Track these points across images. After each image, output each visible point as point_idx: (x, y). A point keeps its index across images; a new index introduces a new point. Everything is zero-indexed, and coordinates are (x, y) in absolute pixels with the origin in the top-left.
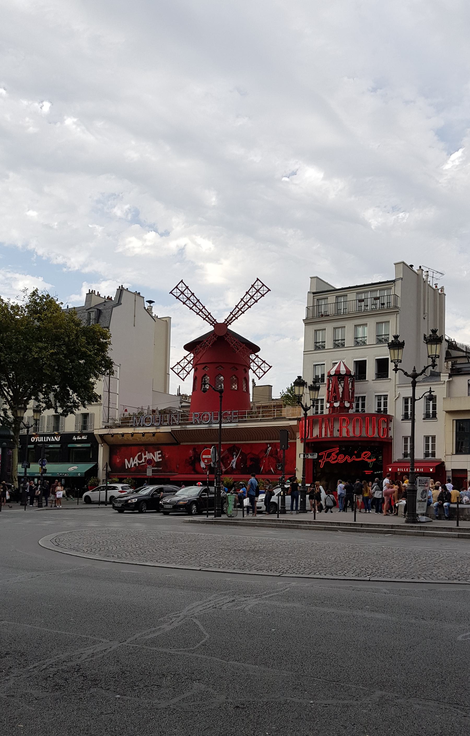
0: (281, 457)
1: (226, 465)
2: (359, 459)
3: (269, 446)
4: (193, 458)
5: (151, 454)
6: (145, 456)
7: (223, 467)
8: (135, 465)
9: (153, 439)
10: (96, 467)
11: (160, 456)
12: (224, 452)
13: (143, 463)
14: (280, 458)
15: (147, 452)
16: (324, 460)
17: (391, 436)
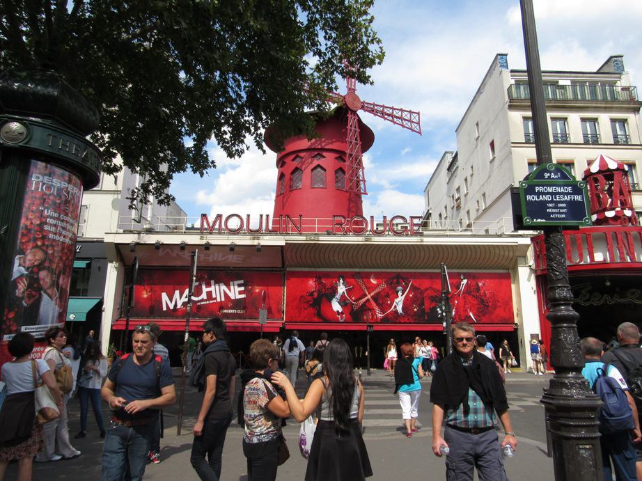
0: (485, 296)
3: (462, 277)
4: (316, 294)
5: (223, 287)
6: (209, 289)
9: (233, 260)
10: (101, 303)
12: (377, 286)
13: (202, 300)
15: (212, 282)
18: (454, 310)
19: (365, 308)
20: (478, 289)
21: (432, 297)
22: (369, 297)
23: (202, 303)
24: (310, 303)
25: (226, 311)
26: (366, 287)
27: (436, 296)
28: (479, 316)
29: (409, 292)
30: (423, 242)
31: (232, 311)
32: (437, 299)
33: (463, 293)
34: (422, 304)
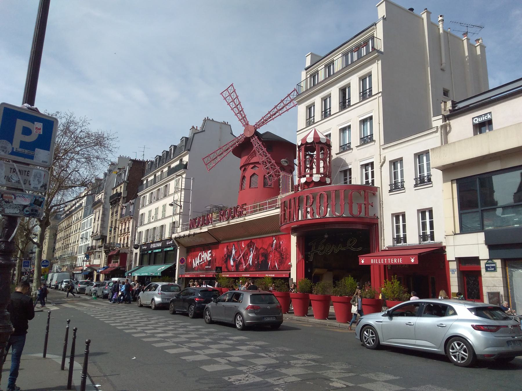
0: (283, 251)
1: (246, 261)
4: (226, 256)
8: (198, 263)
10: (175, 266)
11: (210, 255)
13: (202, 262)
16: (313, 252)
17: (375, 215)
20: (280, 247)
21: (262, 253)
22: (241, 255)
23: (201, 263)
28: (279, 266)
30: (245, 220)
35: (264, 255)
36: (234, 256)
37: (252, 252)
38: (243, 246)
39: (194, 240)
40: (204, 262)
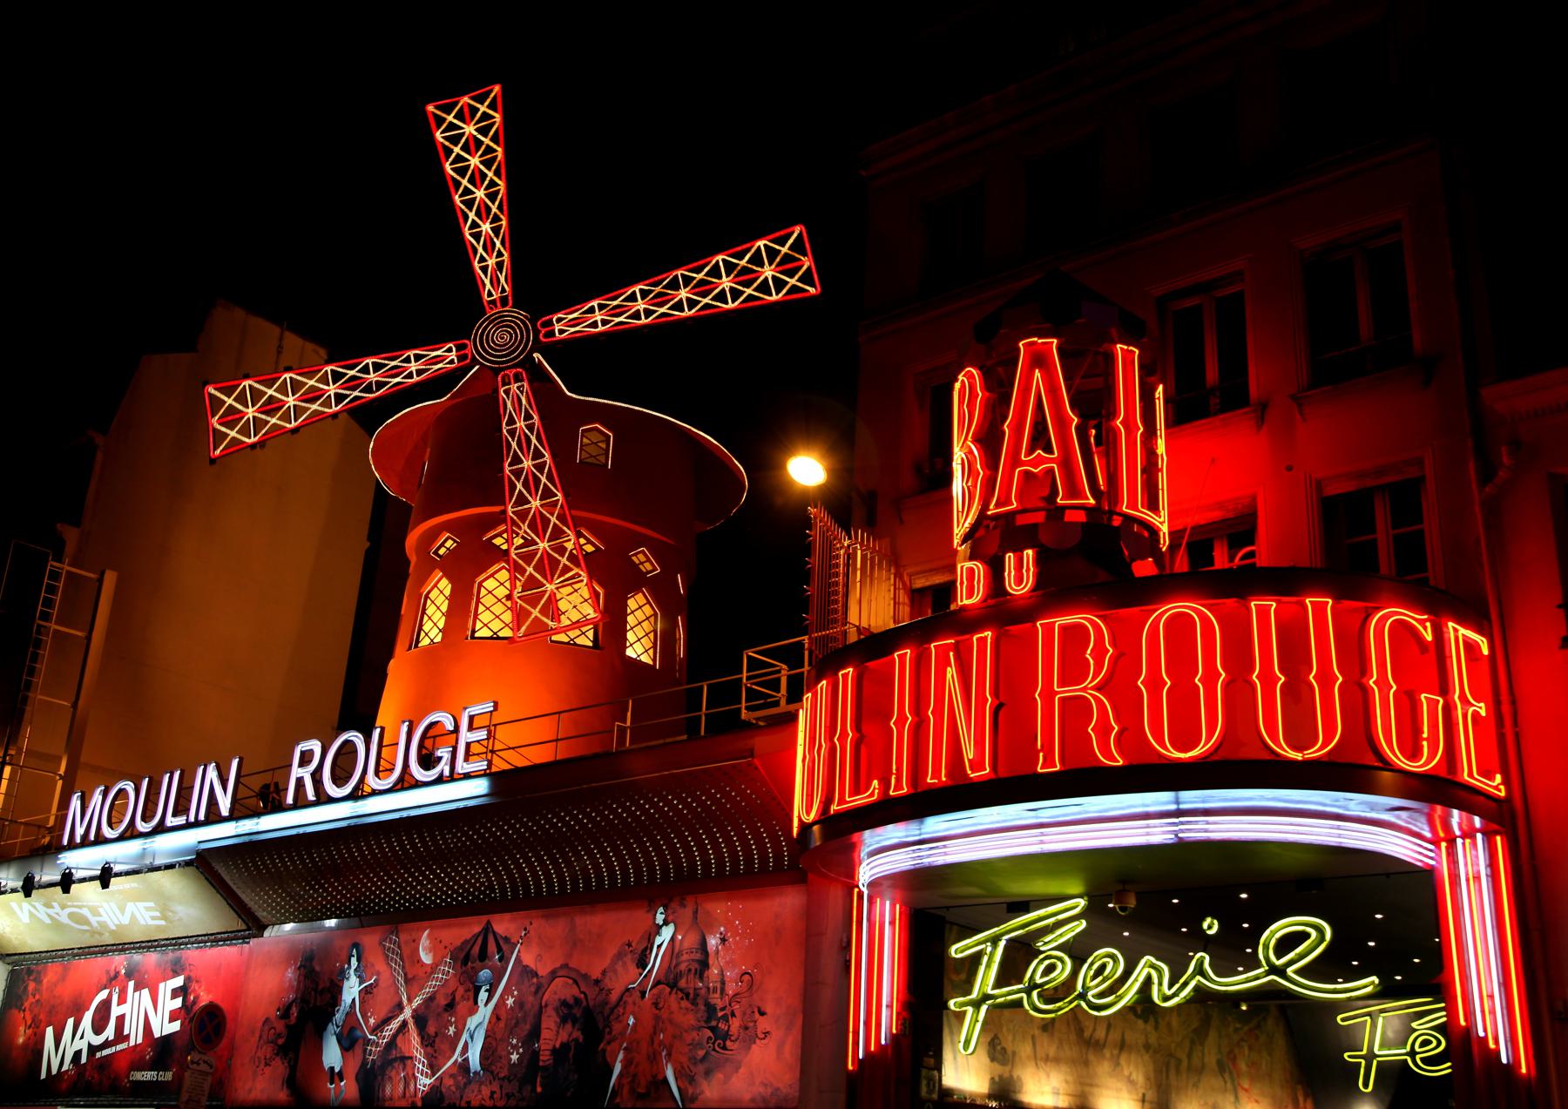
0: (723, 990)
1: (437, 1045)
2: (1237, 983)
3: (660, 918)
7: (421, 1063)
8: (78, 1054)
11: (178, 1003)
12: (434, 968)
13: (106, 1044)
14: (716, 999)
18: (621, 1056)
19: (394, 1054)
20: (704, 964)
21: (564, 1003)
22: (407, 1013)
23: (106, 1052)
24: (281, 1042)
25: (139, 1076)
26: (405, 975)
27: (577, 1001)
29: (507, 991)
31: (149, 1076)
32: (578, 1015)
33: (657, 983)
34: (535, 1034)
35: (577, 1012)
36: (350, 1014)
37: (491, 993)
38: (426, 958)
39: (85, 912)
40: (120, 1047)
